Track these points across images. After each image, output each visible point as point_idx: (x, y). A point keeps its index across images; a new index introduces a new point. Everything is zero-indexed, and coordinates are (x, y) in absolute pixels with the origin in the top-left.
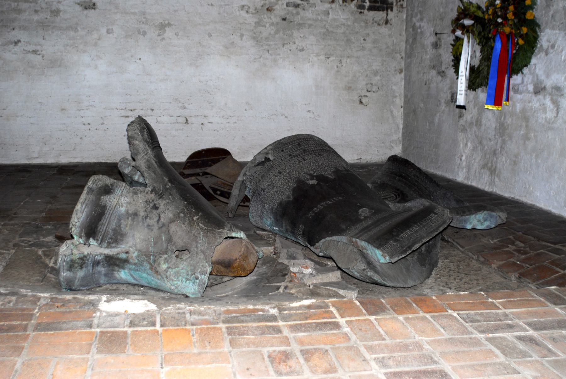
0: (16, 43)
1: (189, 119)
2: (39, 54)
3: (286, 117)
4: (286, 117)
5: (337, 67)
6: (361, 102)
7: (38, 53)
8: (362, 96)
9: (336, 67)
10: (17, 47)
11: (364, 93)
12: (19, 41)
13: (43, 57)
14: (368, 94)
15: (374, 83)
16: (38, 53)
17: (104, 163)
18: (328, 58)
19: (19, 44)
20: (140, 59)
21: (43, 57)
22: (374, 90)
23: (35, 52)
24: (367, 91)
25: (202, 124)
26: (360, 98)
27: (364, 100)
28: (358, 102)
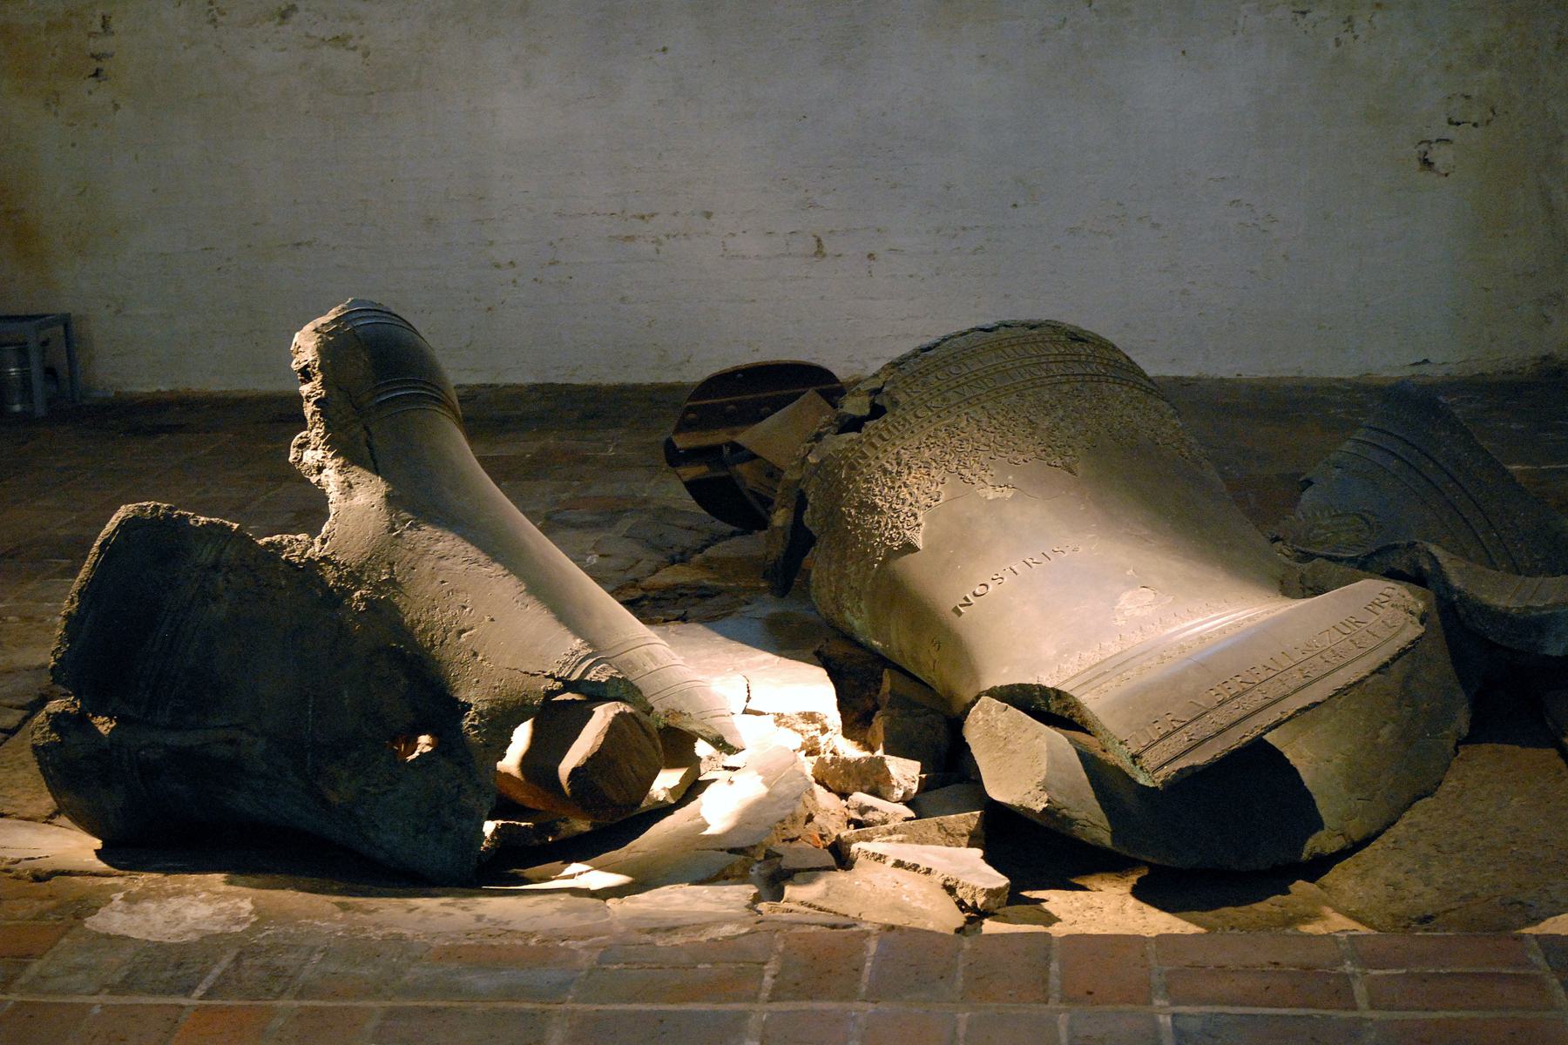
0: (284, 16)
1: (824, 241)
2: (355, 49)
3: (1156, 226)
4: (1156, 226)
5: (1338, 43)
6: (1427, 163)
7: (351, 44)
8: (1430, 142)
9: (1331, 43)
10: (289, 28)
11: (1440, 129)
12: (293, 8)
13: (366, 55)
14: (1452, 132)
15: (1475, 93)
16: (351, 44)
17: (534, 388)
18: (1304, 13)
19: (295, 18)
20: (664, 50)
21: (366, 55)
22: (1475, 118)
23: (340, 41)
24: (1450, 122)
25: (870, 256)
26: (1424, 147)
27: (1440, 156)
28: (1417, 165)
